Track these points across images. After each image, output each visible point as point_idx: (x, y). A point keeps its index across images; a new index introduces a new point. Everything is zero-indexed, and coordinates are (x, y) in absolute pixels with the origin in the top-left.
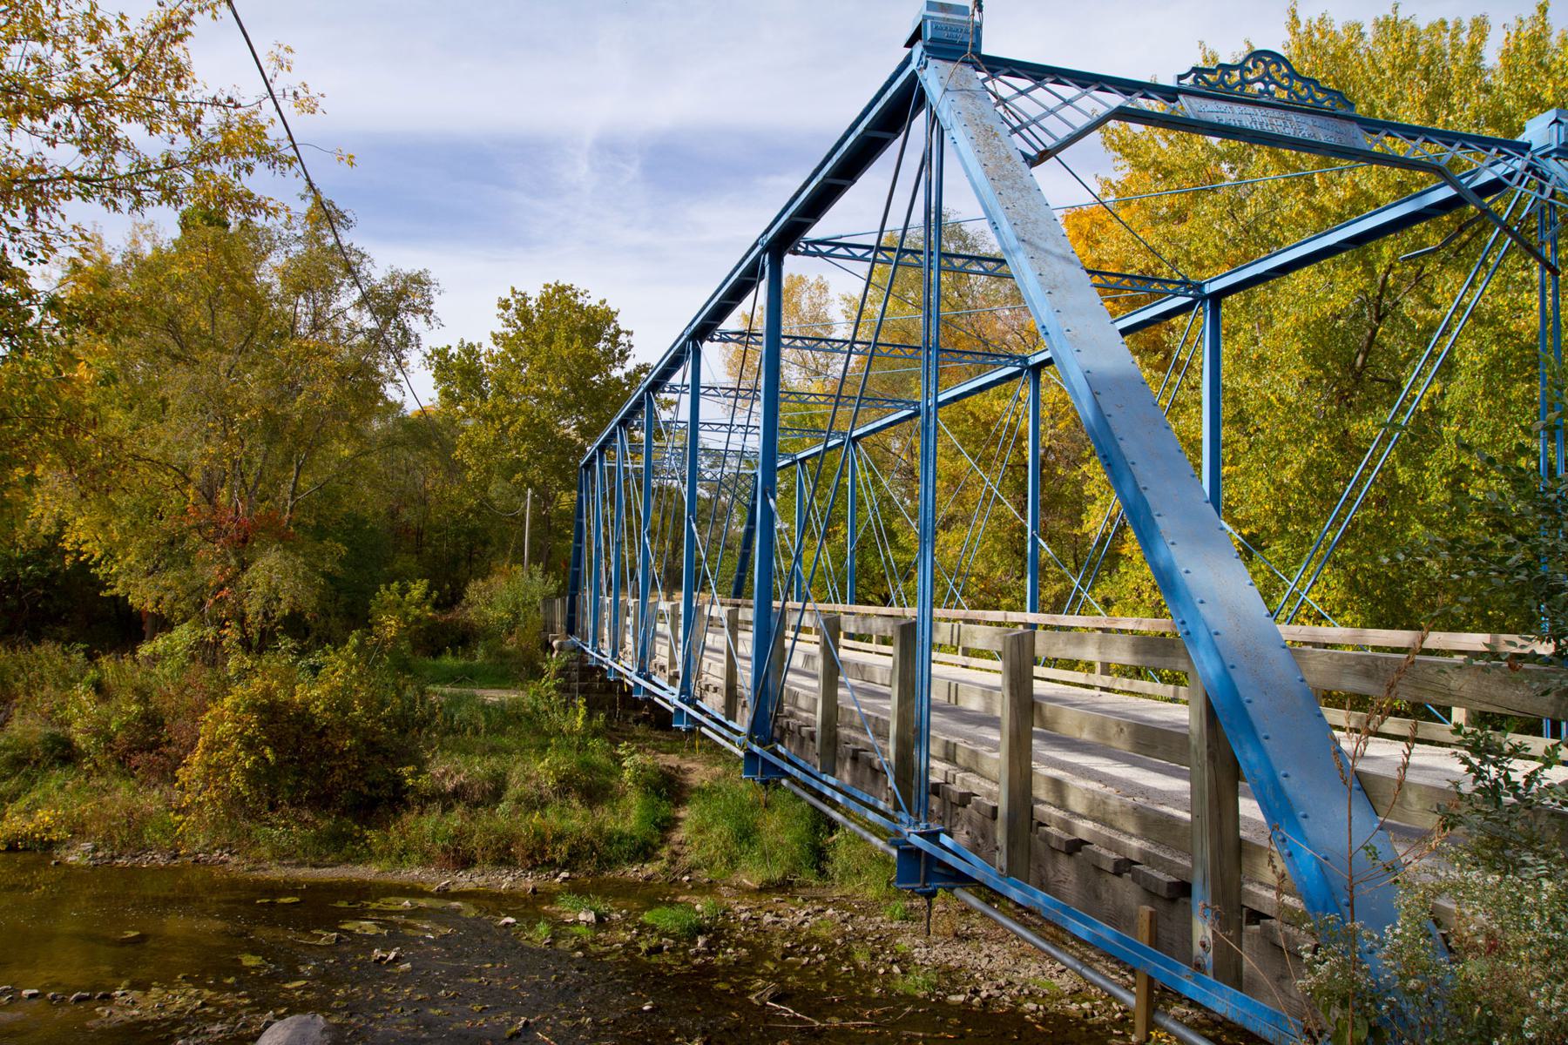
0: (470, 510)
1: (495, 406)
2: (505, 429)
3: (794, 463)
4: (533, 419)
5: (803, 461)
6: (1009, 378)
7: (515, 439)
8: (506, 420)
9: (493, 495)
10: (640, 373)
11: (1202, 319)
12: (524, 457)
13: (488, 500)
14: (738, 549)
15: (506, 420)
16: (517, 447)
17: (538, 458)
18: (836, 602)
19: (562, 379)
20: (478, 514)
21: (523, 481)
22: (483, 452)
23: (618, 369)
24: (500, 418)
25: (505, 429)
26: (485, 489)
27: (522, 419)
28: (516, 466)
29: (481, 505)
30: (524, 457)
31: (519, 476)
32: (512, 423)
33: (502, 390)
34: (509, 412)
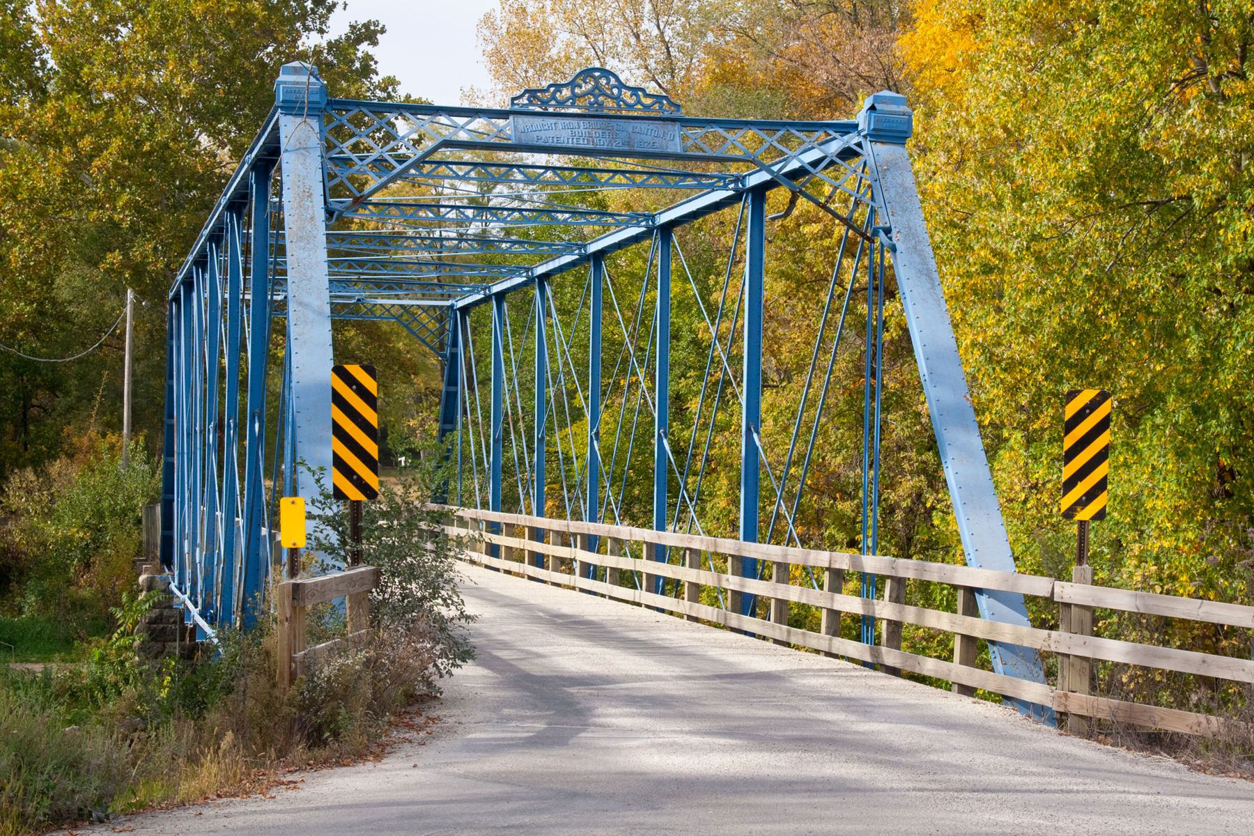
0: (18, 325)
1: (61, 115)
2: (81, 163)
3: (486, 299)
4: (139, 144)
5: (500, 296)
6: (636, 239)
7: (106, 181)
8: (86, 143)
9: (65, 294)
10: (359, 41)
11: (741, 211)
12: (126, 220)
13: (54, 302)
14: (764, 344)
15: (86, 143)
16: (112, 197)
17: (153, 221)
18: (530, 513)
19: (193, 63)
20: (35, 330)
21: (124, 266)
22: (41, 208)
23: (314, 34)
24: (72, 140)
25: (81, 163)
26: (47, 282)
27: (116, 143)
28: (109, 236)
29: (41, 312)
30: (126, 220)
31: (115, 257)
32: (98, 150)
33: (74, 81)
34: (89, 128)
